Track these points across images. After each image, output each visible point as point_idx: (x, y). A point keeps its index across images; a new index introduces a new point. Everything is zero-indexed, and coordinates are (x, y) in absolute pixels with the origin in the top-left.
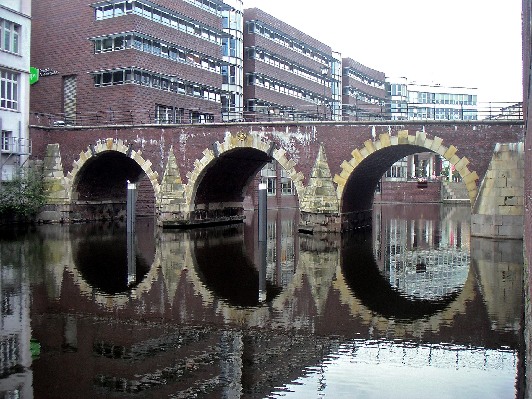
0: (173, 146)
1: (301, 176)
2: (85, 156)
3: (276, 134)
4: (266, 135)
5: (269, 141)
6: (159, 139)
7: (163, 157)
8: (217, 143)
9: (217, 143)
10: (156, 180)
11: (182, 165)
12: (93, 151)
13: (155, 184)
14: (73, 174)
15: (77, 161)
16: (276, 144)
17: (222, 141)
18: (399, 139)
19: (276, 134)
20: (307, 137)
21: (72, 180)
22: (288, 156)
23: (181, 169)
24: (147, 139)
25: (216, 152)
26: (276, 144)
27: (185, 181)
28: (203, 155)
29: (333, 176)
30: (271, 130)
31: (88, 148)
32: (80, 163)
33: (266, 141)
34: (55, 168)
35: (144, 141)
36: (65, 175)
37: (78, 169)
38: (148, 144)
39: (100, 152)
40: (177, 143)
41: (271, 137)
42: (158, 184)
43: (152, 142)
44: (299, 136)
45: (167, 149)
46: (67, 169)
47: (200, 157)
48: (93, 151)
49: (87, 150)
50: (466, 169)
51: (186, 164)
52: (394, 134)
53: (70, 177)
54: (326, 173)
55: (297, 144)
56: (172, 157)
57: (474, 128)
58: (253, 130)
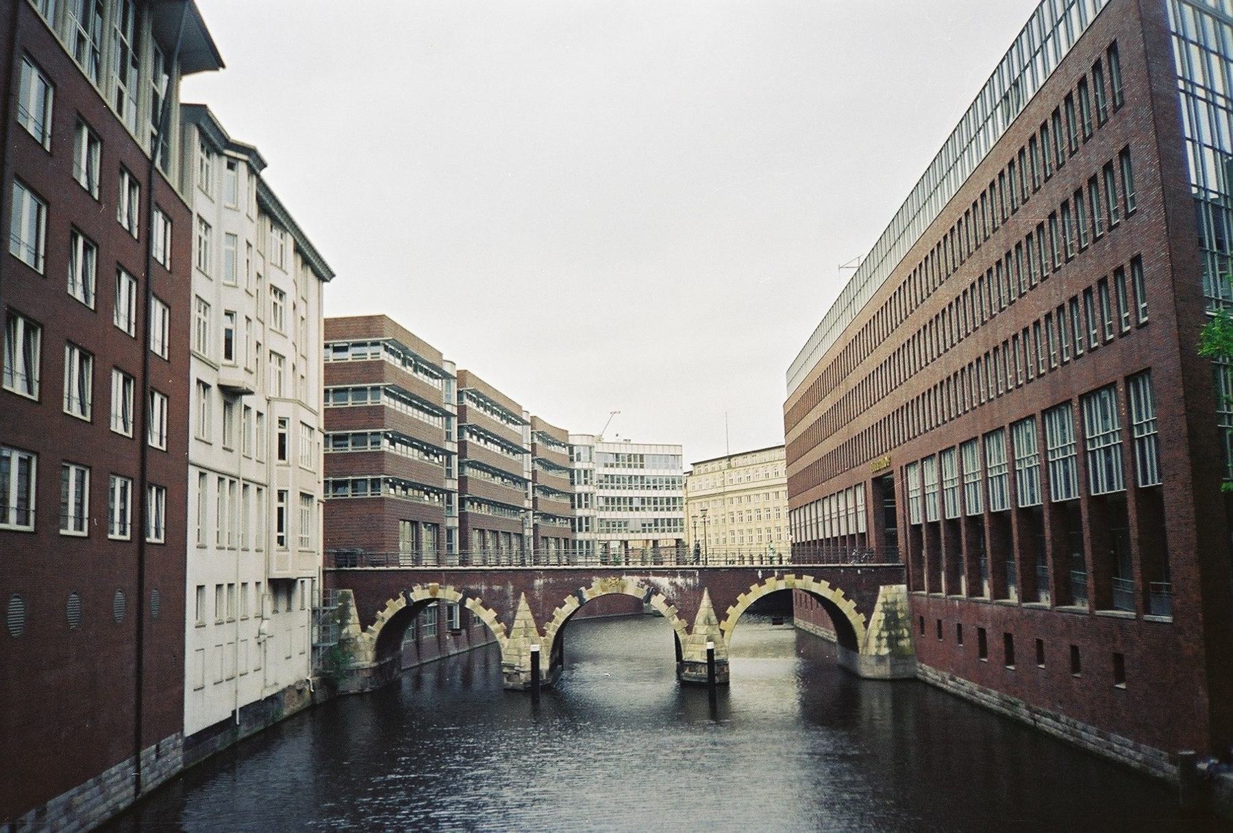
0: (526, 593)
1: (684, 623)
2: (395, 606)
3: (652, 578)
4: (642, 581)
5: (646, 587)
6: (504, 584)
7: (512, 606)
8: (583, 589)
9: (583, 589)
10: (503, 633)
11: (537, 615)
12: (408, 600)
13: (500, 638)
14: (376, 628)
15: (382, 611)
16: (655, 590)
17: (588, 587)
18: (786, 583)
19: (652, 578)
20: (690, 581)
21: (375, 636)
22: (668, 602)
23: (536, 619)
24: (489, 584)
25: (581, 600)
26: (655, 590)
27: (542, 633)
28: (565, 603)
29: (719, 623)
30: (647, 574)
31: (401, 595)
32: (388, 614)
33: (642, 587)
34: (350, 621)
35: (484, 588)
36: (364, 629)
37: (385, 623)
38: (489, 591)
39: (418, 600)
40: (529, 590)
41: (648, 582)
42: (505, 638)
43: (496, 588)
44: (679, 580)
45: (517, 596)
46: (366, 623)
47: (561, 605)
48: (408, 600)
49: (399, 597)
50: (854, 612)
51: (543, 614)
52: (780, 578)
53: (372, 632)
54: (713, 618)
55: (679, 589)
56: (523, 604)
57: (859, 572)
58: (627, 575)
